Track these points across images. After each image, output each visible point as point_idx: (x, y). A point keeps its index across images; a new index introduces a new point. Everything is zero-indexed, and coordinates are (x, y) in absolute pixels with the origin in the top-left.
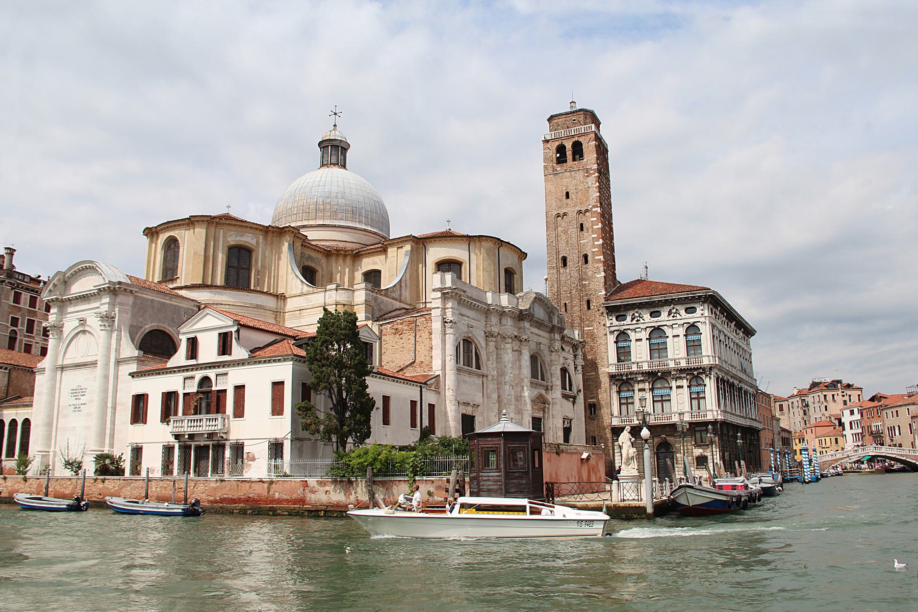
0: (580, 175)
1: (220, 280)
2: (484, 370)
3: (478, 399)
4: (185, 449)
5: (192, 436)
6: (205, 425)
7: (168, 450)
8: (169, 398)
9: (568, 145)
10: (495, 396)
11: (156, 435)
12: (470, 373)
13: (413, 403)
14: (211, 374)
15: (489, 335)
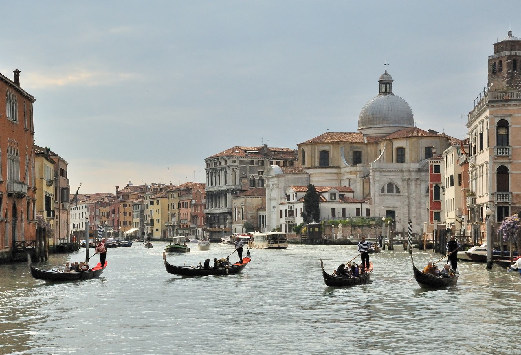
0: (500, 80)
1: (317, 164)
2: (401, 194)
3: (398, 204)
4: (289, 225)
5: (289, 222)
6: (290, 219)
7: (286, 225)
8: (286, 211)
9: (497, 62)
10: (406, 203)
11: (283, 221)
12: (391, 196)
13: (358, 210)
14: (292, 205)
15: (403, 180)
